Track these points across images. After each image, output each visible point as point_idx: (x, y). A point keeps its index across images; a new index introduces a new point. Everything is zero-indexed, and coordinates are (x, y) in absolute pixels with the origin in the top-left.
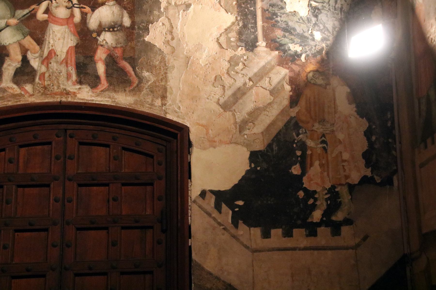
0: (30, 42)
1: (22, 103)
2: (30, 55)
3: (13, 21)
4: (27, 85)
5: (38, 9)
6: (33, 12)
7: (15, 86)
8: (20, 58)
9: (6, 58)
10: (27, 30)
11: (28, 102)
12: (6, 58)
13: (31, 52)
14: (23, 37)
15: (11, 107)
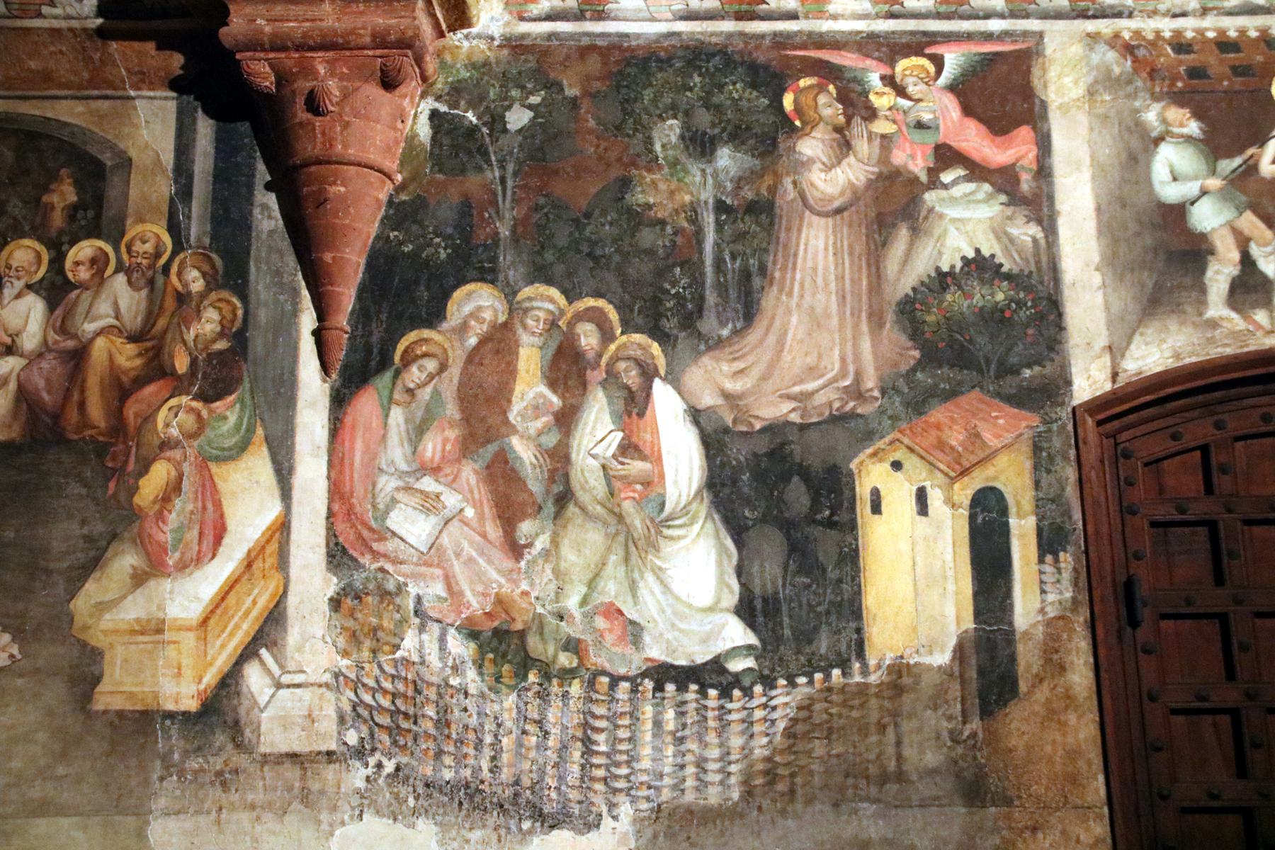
0: (1252, 223)
1: (1252, 348)
2: (1255, 250)
3: (1214, 183)
4: (1257, 311)
5: (1260, 156)
6: (1251, 162)
7: (1234, 315)
8: (1236, 256)
9: (1210, 258)
10: (1244, 198)
11: (1263, 348)
12: (1210, 258)
13: (1259, 245)
14: (1236, 214)
15: (1235, 357)
